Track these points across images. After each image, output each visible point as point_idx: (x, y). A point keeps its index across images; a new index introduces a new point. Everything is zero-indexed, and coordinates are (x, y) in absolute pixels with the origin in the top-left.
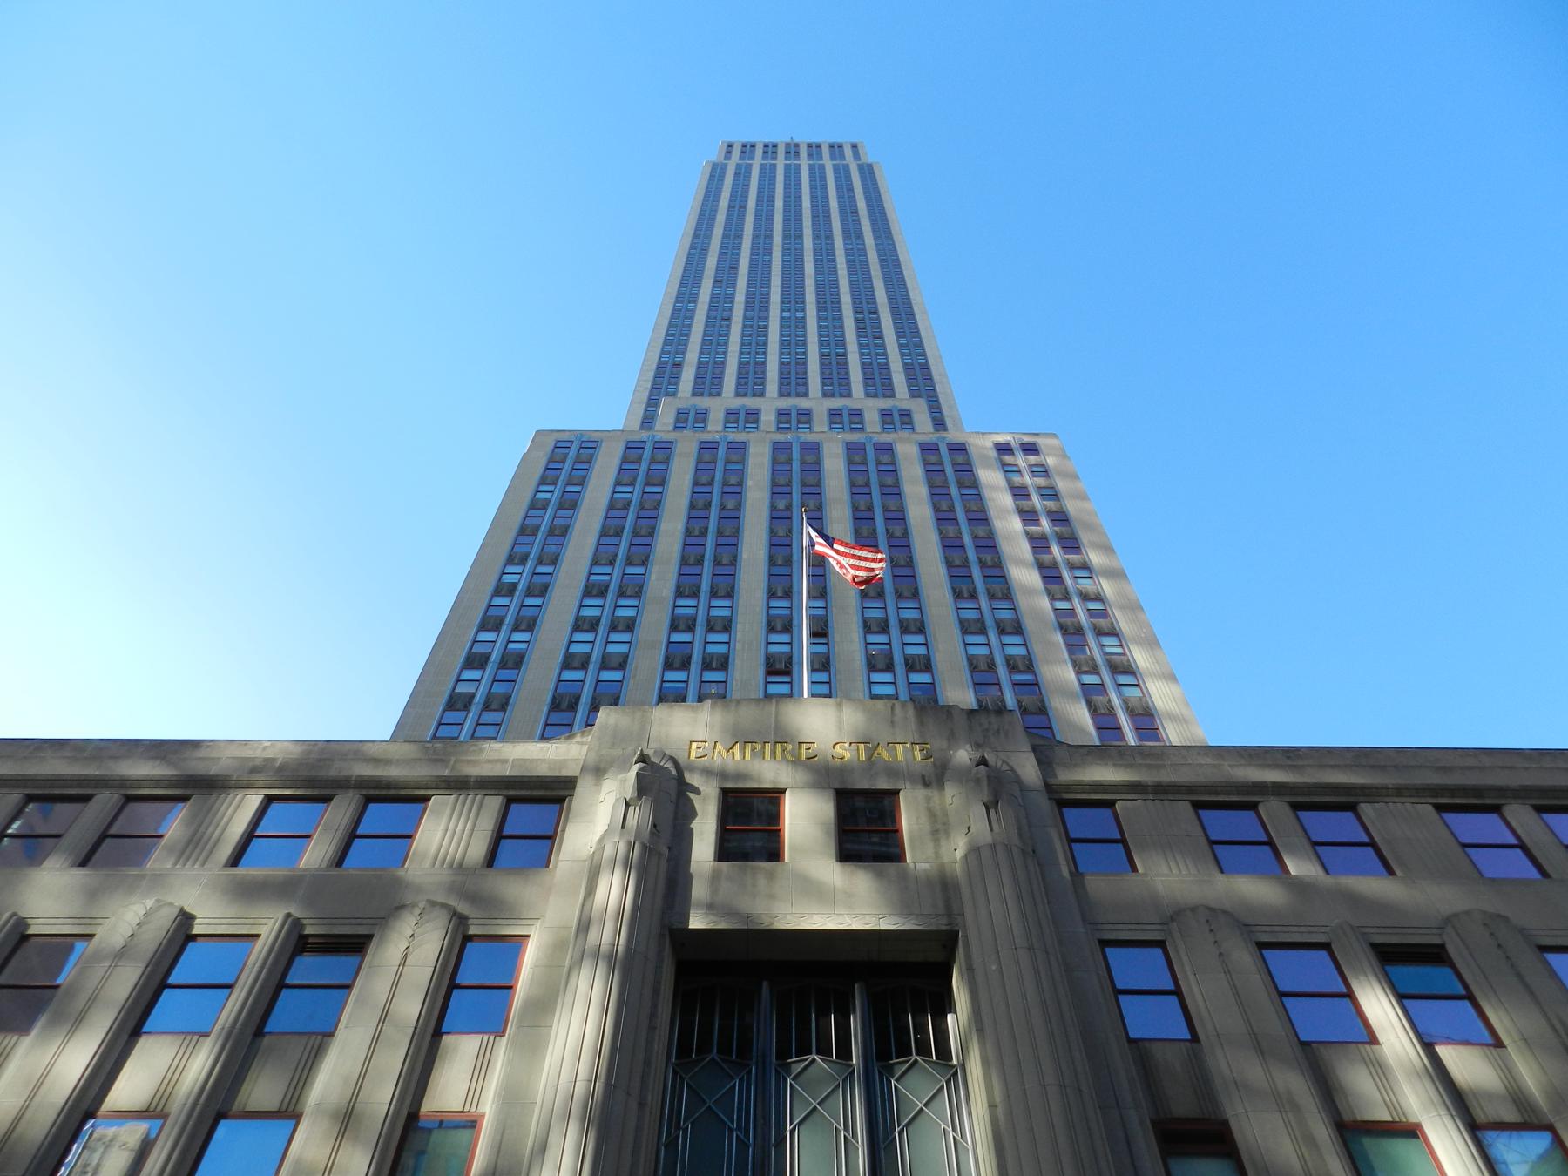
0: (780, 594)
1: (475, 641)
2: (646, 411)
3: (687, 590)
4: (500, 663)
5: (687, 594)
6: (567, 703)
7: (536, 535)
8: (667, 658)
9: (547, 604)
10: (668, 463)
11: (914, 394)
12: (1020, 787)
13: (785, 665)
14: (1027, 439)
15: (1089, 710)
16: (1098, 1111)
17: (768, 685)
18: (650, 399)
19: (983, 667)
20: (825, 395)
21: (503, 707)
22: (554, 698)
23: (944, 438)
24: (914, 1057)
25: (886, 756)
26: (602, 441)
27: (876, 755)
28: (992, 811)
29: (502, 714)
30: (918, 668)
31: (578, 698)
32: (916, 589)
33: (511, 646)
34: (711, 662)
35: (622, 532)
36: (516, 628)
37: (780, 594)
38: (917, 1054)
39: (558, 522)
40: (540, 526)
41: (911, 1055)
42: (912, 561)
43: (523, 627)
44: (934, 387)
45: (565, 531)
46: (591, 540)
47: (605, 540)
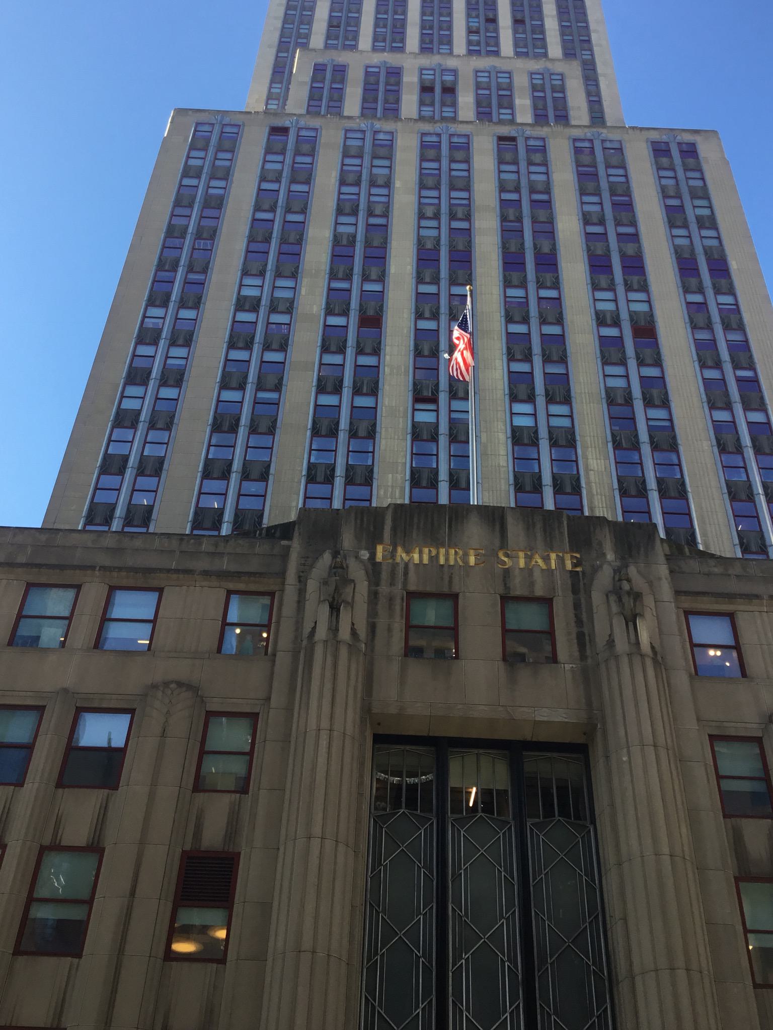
0: (427, 315)
1: (134, 355)
2: (277, 57)
3: (337, 308)
4: (161, 380)
5: (336, 312)
6: (227, 424)
7: (184, 238)
8: (319, 380)
9: (202, 316)
10: (313, 156)
11: (569, 54)
12: (655, 599)
13: (432, 392)
14: (688, 138)
15: (718, 448)
16: (696, 871)
17: (416, 413)
18: (280, 42)
19: (620, 400)
20: (470, 52)
21: (168, 427)
22: (215, 418)
23: (599, 134)
24: (557, 818)
25: (544, 567)
26: (244, 125)
27: (533, 563)
28: (631, 625)
29: (167, 433)
30: (558, 400)
31: (238, 420)
32: (561, 314)
33: (169, 361)
34: (361, 387)
35: (270, 238)
36: (173, 343)
37: (427, 315)
38: (559, 816)
39: (205, 222)
40: (187, 227)
41: (554, 816)
42: (558, 283)
43: (181, 342)
44: (589, 36)
45: (213, 234)
46: (240, 245)
47: (253, 247)
